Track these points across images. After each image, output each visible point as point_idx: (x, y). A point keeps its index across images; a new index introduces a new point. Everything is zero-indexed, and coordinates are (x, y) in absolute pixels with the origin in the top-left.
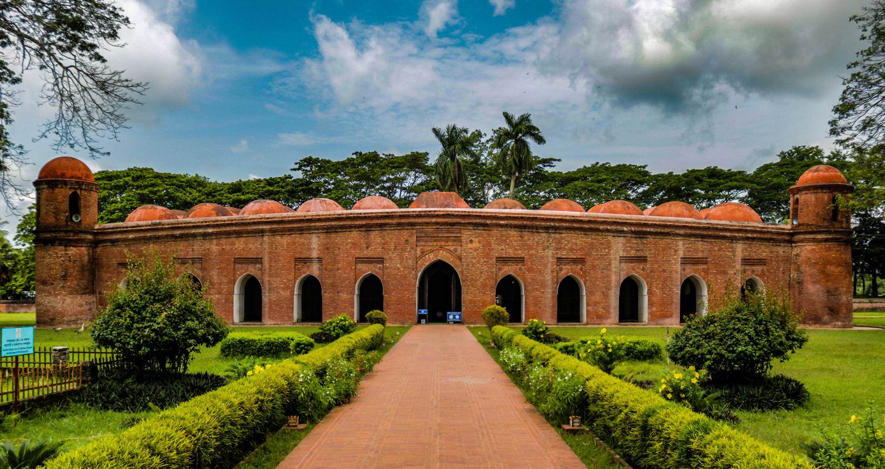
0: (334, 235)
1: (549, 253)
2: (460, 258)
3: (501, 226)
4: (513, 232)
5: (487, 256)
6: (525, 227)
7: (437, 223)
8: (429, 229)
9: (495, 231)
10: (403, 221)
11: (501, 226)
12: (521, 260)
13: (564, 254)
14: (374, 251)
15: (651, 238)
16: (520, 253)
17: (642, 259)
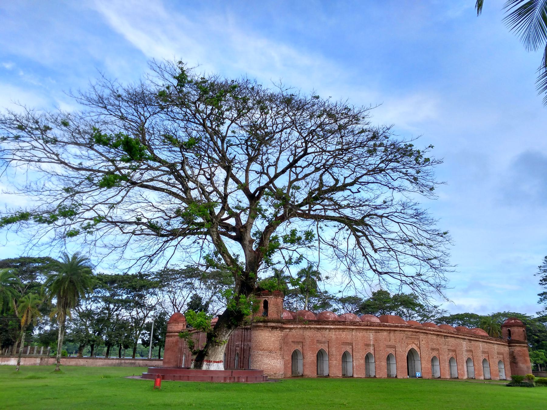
0: (378, 334)
1: (446, 347)
2: (420, 348)
3: (432, 334)
4: (435, 337)
5: (428, 347)
6: (438, 335)
7: (412, 331)
8: (410, 333)
9: (430, 336)
10: (401, 329)
11: (432, 334)
12: (438, 350)
13: (450, 348)
14: (392, 343)
15: (473, 342)
16: (438, 347)
17: (471, 351)
